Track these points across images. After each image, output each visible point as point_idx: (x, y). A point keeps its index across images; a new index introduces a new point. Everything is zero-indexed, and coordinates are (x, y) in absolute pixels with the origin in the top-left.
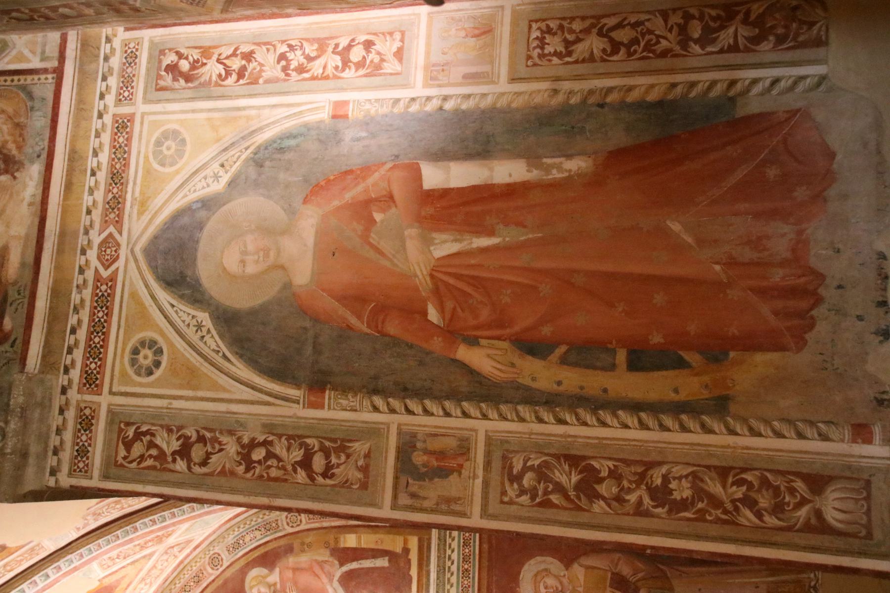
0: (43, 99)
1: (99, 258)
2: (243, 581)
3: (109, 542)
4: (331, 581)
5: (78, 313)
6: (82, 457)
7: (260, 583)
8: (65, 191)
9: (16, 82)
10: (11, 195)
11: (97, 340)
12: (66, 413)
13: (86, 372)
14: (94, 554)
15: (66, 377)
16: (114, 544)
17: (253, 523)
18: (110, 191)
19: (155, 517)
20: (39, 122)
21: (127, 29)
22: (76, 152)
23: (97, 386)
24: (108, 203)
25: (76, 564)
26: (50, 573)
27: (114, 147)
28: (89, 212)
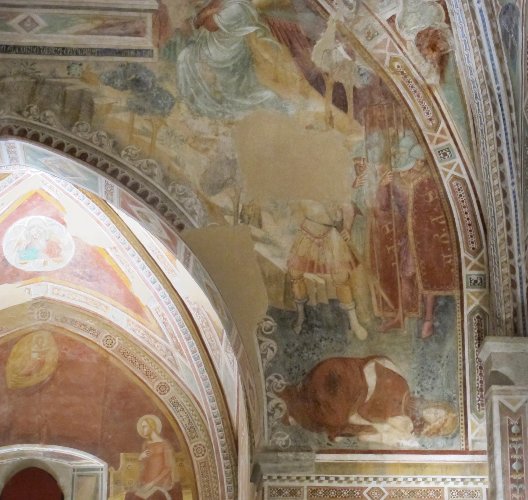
0: (452, 444)
1: (373, 488)
2: (150, 413)
3: (178, 321)
4: (157, 485)
5: (345, 480)
6: (277, 493)
7: (151, 427)
8: (405, 464)
9: (461, 426)
10: (402, 432)
11: (333, 493)
12: (297, 481)
13: (317, 490)
14: (170, 312)
15: (314, 478)
16: (177, 325)
17: (194, 417)
18: (406, 490)
19: (198, 353)
20: (441, 443)
21: (487, 490)
22: (425, 467)
23: (311, 496)
24: (399, 490)
25: (163, 301)
26: (156, 284)
27: (427, 490)
28: (395, 479)
